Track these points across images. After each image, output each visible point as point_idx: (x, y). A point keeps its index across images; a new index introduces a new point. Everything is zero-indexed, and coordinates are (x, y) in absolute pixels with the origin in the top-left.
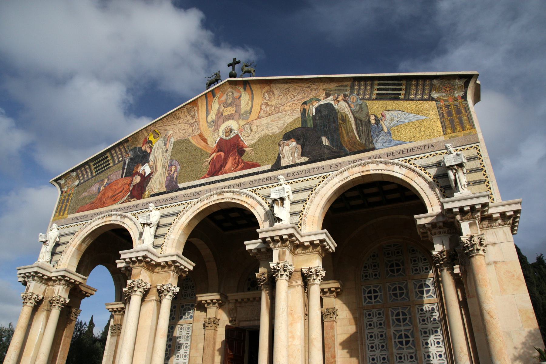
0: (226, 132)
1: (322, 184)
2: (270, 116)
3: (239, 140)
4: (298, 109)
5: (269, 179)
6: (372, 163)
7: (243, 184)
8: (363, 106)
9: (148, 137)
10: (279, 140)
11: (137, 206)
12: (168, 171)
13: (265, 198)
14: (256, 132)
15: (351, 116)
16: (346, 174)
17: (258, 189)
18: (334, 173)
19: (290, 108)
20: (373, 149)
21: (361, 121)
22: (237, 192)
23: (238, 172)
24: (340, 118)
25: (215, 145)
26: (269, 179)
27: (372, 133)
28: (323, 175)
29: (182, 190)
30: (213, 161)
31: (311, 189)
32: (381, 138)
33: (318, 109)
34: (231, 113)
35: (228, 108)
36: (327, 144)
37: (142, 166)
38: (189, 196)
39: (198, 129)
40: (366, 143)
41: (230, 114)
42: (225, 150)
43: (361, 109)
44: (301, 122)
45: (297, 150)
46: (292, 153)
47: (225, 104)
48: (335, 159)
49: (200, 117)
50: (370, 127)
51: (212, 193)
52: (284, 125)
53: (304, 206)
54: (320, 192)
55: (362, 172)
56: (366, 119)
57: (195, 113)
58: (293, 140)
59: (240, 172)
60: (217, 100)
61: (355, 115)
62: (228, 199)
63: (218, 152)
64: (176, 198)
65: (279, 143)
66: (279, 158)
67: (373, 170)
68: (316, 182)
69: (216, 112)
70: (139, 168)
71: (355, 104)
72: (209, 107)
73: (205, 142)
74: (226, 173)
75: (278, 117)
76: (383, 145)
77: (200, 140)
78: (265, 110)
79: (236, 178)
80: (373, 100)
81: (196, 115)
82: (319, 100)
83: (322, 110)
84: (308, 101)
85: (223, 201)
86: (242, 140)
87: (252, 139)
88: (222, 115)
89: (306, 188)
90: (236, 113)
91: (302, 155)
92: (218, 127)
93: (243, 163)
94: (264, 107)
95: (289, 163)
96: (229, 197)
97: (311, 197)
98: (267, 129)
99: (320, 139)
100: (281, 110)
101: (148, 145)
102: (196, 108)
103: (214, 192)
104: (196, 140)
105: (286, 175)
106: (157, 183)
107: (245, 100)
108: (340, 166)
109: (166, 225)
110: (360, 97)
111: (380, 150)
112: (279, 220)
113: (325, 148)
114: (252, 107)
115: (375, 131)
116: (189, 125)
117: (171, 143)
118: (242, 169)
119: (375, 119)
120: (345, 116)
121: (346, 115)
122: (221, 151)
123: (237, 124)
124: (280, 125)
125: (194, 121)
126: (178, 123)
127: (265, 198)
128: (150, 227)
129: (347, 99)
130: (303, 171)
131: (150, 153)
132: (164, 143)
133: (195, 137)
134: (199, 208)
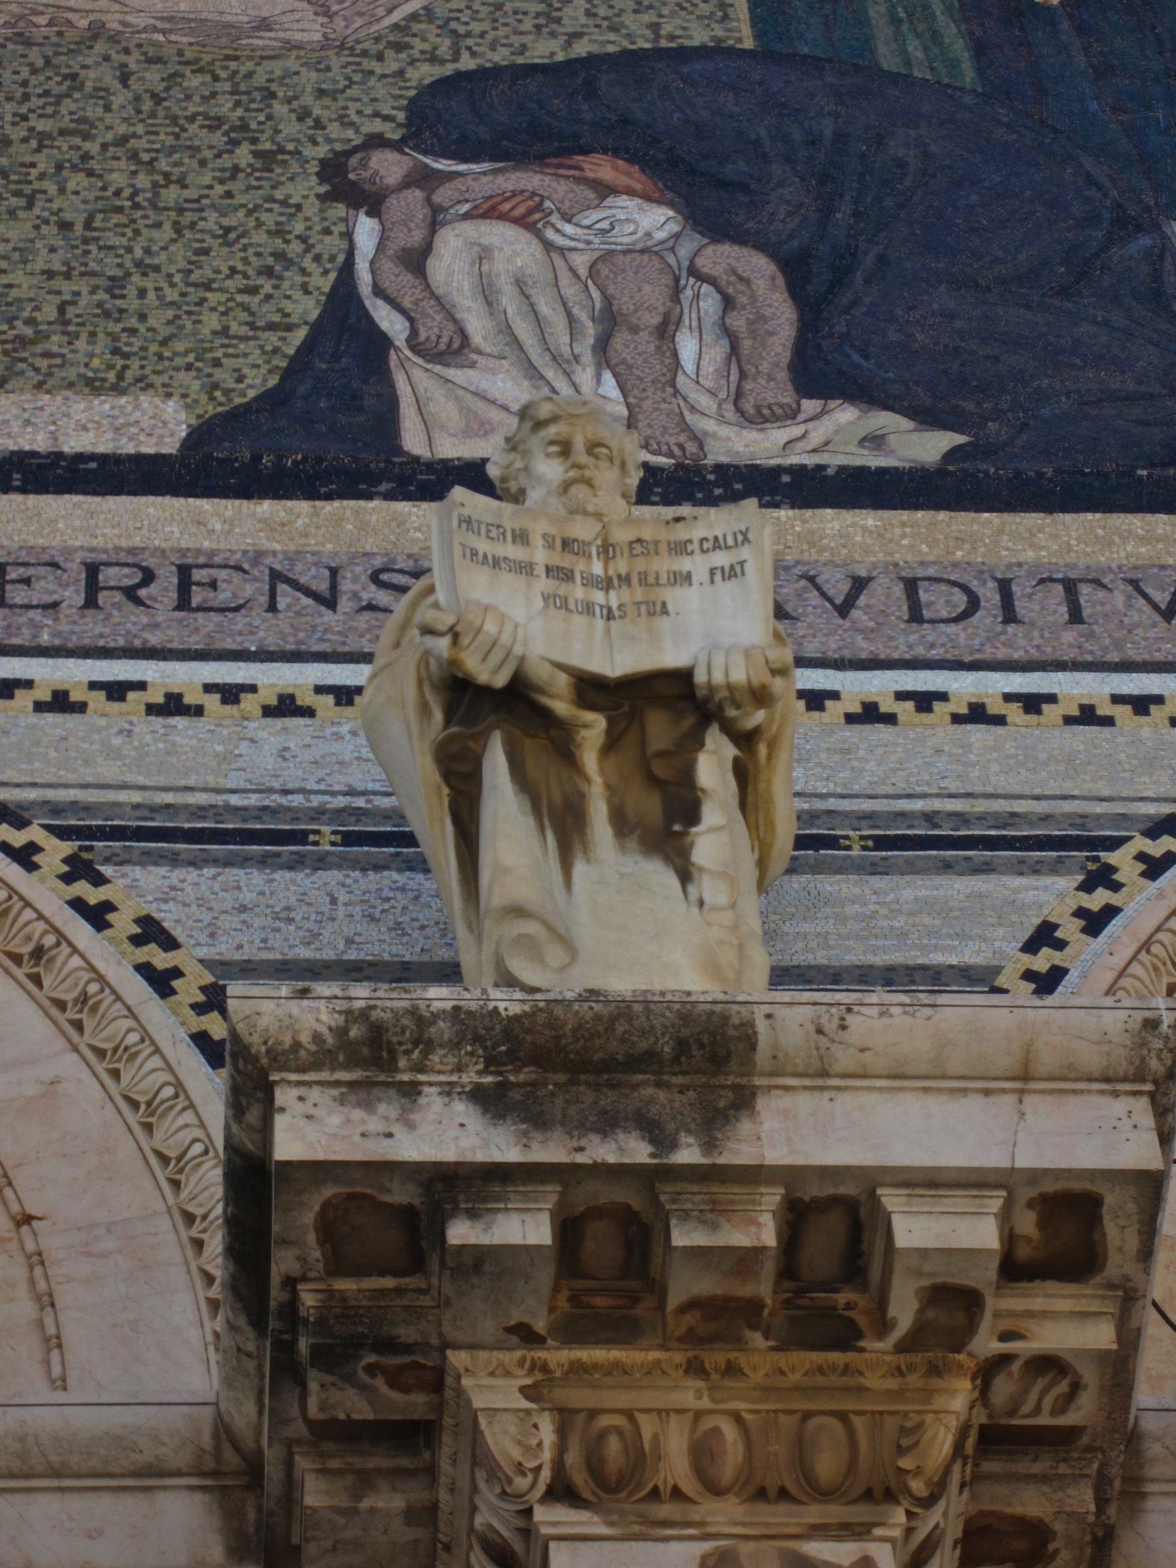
5: (164, 590)
13: (55, 852)
45: (710, 303)
58: (603, 168)
89: (962, 818)
99: (1145, 241)
127: (55, 852)
130: (859, 584)
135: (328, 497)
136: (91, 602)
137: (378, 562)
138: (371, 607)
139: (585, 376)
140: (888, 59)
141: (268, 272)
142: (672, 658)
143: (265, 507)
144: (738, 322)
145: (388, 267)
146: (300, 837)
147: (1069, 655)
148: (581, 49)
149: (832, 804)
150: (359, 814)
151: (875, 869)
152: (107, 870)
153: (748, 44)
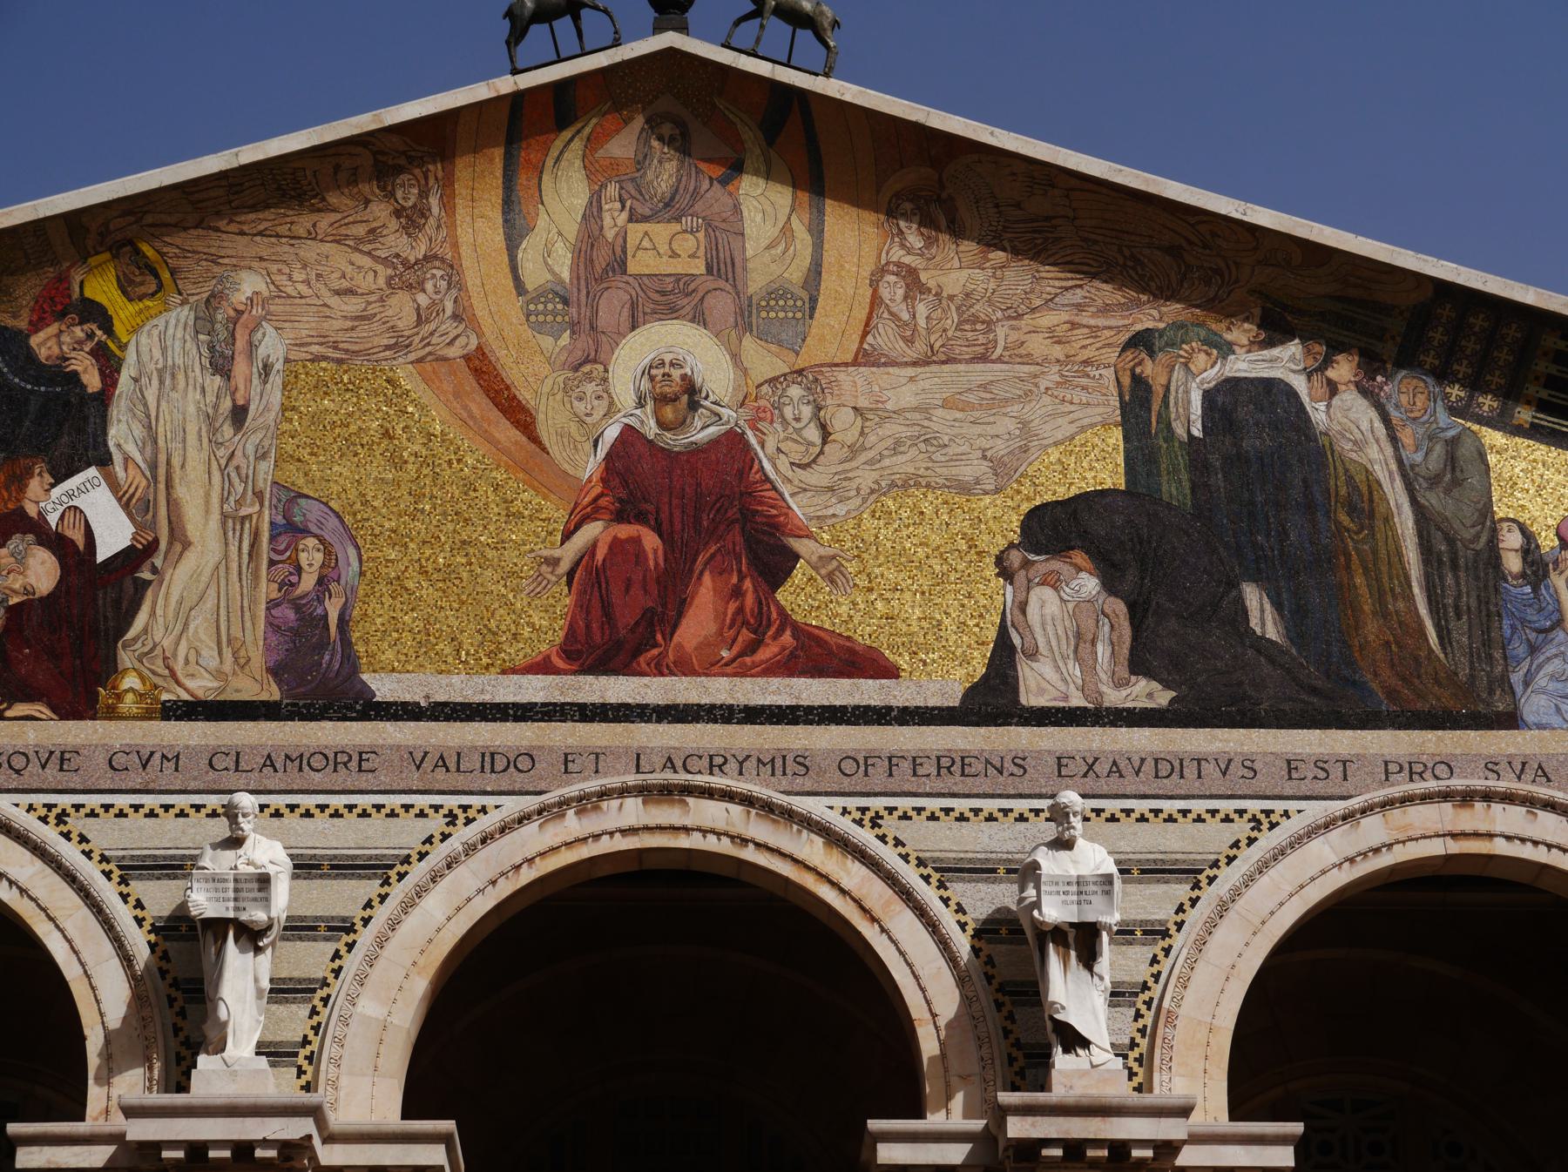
0: (662, 400)
1: (1249, 858)
2: (934, 368)
3: (754, 476)
4: (1102, 372)
5: (956, 769)
6: (1509, 798)
7: (803, 762)
8: (1465, 451)
9: (78, 279)
10: (1002, 543)
11: (63, 758)
12: (272, 563)
13: (935, 876)
14: (854, 451)
15: (1396, 494)
16: (1373, 829)
17: (891, 810)
18: (1316, 811)
19: (1058, 352)
20: (1511, 720)
21: (1450, 541)
22: (768, 809)
23: (761, 681)
24: (1343, 491)
25: (590, 466)
26: (956, 769)
27: (1507, 632)
28: (1254, 806)
29: (396, 718)
30: (588, 570)
31: (1192, 873)
32: (1549, 668)
33: (1220, 399)
34: (678, 267)
35: (661, 232)
36: (1272, 633)
37: (59, 479)
38: (452, 766)
39: (456, 317)
40: (1472, 677)
41: (678, 277)
42: (664, 516)
43: (1453, 470)
44: (1121, 460)
45: (1107, 628)
46: (1082, 641)
47: (630, 187)
48: (1315, 734)
49: (464, 235)
50: (1497, 590)
51: (613, 781)
52: (1025, 450)
53: (1154, 961)
54: (1241, 903)
55: (1454, 836)
56: (1477, 536)
57: (424, 194)
58: (1079, 557)
59: (775, 682)
60: (577, 145)
61: (1422, 501)
62: (712, 838)
63: (620, 517)
64: (362, 759)
65: (999, 560)
66: (1004, 656)
67: (1509, 838)
68: (1215, 838)
69: (572, 229)
70: (35, 486)
71: (1421, 431)
72: (522, 179)
73: (517, 424)
74: (684, 668)
75: (984, 387)
76: (1558, 710)
77: (480, 405)
78: (905, 316)
79: (754, 715)
80: (1517, 431)
81: (435, 210)
82: (1226, 349)
83: (1241, 413)
84: (1162, 333)
85: (683, 842)
86: (767, 479)
87: (831, 489)
88: (623, 265)
90: (711, 283)
91: (1139, 664)
92: (597, 344)
93: (788, 633)
94: (893, 290)
95: (1066, 698)
96: (720, 825)
97: (1194, 917)
98: (922, 446)
99: (1234, 593)
100: (1001, 344)
101: (79, 332)
102: (436, 169)
103: (632, 779)
104: (457, 395)
105: (1052, 761)
106: (200, 625)
107: (769, 209)
108: (1340, 774)
109: (314, 928)
110: (1447, 396)
111: (1546, 733)
112: (1074, 1040)
113: (1259, 652)
114: (815, 271)
115: (1523, 621)
116: (384, 272)
117: (267, 368)
118: (788, 666)
119: (1529, 549)
120: (1365, 490)
121: (1373, 485)
122: (641, 518)
123: (725, 360)
124: (1000, 448)
125: (421, 250)
126: (302, 232)
127: (935, 876)
128: (258, 950)
129: (1381, 389)
130: (1143, 760)
131: (104, 398)
132: (211, 348)
133: (443, 369)
134: (530, 861)
135: (1000, 725)
136: (939, 774)
137: (1013, 754)
138: (1012, 774)
139: (1071, 663)
140: (1165, 497)
141: (981, 616)
142: (1091, 918)
143: (983, 730)
144: (1115, 639)
145: (1017, 612)
146: (994, 871)
147: (1196, 792)
148: (1074, 491)
149: (1131, 856)
150: (1010, 861)
151: (1140, 882)
152: (948, 884)
153: (1123, 487)
